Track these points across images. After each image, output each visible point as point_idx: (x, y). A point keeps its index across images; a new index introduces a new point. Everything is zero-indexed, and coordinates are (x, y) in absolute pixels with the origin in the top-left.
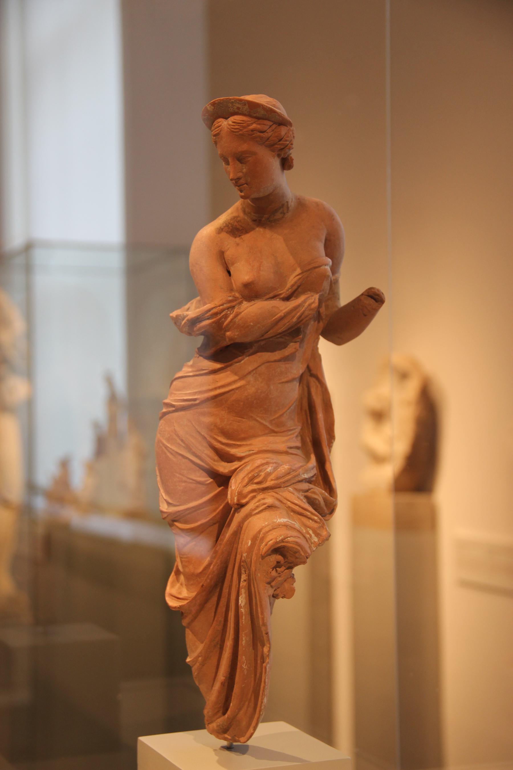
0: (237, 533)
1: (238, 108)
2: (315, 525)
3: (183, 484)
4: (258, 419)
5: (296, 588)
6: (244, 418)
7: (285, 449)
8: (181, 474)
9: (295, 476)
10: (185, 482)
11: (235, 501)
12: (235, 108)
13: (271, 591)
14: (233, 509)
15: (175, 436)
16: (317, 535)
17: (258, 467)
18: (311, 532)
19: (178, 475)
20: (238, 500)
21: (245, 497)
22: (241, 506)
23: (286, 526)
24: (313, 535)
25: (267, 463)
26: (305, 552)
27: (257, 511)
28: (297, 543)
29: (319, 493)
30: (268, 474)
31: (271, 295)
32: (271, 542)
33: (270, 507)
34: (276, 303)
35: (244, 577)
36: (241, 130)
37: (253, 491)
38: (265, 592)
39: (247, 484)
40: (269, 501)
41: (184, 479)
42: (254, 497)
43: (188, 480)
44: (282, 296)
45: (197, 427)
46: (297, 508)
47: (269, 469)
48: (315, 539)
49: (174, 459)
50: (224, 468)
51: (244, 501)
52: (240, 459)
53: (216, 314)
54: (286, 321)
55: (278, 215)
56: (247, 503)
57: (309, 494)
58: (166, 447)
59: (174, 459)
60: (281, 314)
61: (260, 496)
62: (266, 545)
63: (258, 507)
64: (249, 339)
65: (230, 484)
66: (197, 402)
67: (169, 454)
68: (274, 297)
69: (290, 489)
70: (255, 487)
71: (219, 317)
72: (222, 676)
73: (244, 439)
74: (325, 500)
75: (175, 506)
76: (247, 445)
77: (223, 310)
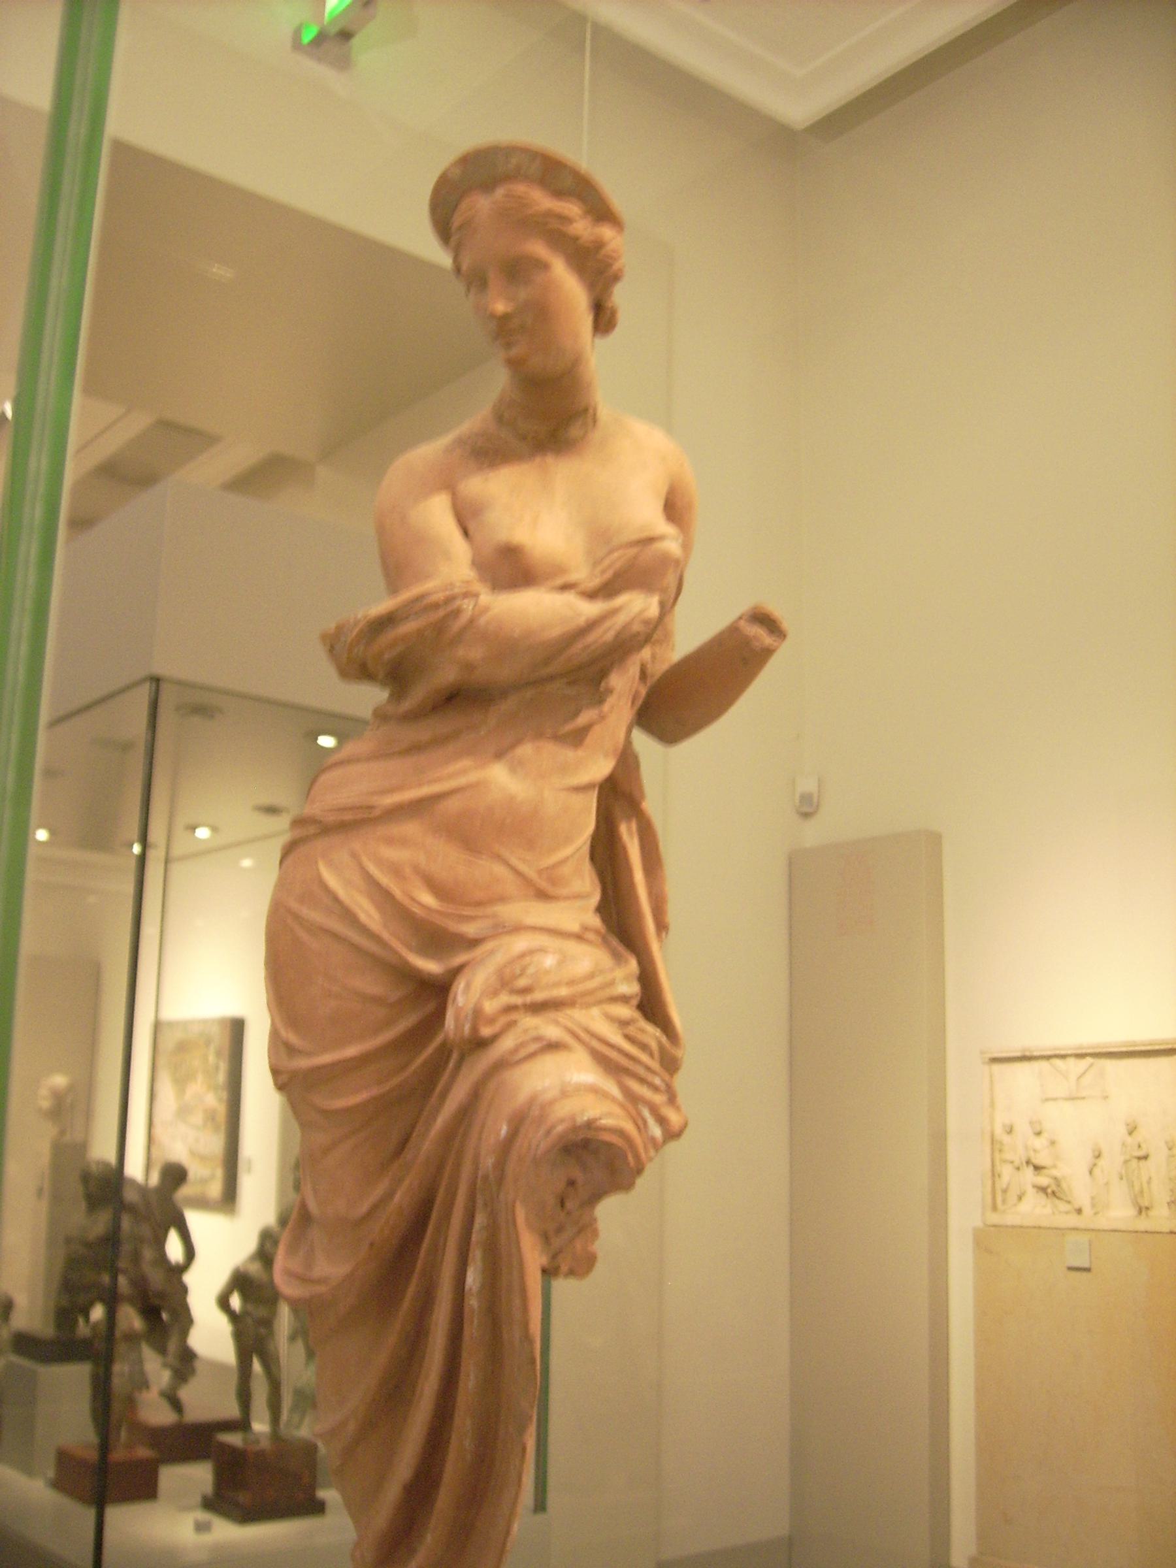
0: (466, 1113)
2: (659, 1099)
4: (514, 861)
5: (600, 1255)
7: (575, 927)
9: (604, 986)
11: (467, 1029)
13: (544, 1260)
14: (455, 1056)
16: (662, 1121)
17: (523, 955)
18: (646, 1113)
20: (475, 1029)
21: (491, 1021)
22: (480, 1044)
23: (594, 1090)
24: (651, 1122)
25: (542, 950)
26: (637, 1157)
28: (621, 1133)
29: (651, 1033)
30: (547, 972)
31: (559, 581)
32: (560, 1128)
33: (553, 1046)
34: (570, 598)
35: (480, 1220)
37: (510, 1009)
38: (533, 1257)
39: (495, 993)
40: (552, 1032)
42: (511, 1025)
44: (582, 587)
46: (614, 1055)
47: (549, 961)
48: (656, 1131)
51: (486, 1031)
52: (474, 943)
53: (436, 606)
54: (591, 638)
55: (575, 431)
56: (494, 1038)
57: (631, 1030)
58: (297, 917)
60: (582, 621)
61: (529, 1022)
62: (548, 1132)
63: (522, 1045)
64: (505, 673)
65: (451, 996)
66: (377, 812)
67: (303, 935)
68: (565, 587)
69: (595, 1011)
70: (517, 1000)
71: (441, 613)
72: (404, 1467)
73: (479, 904)
74: (662, 1048)
75: (309, 1054)
76: (487, 917)
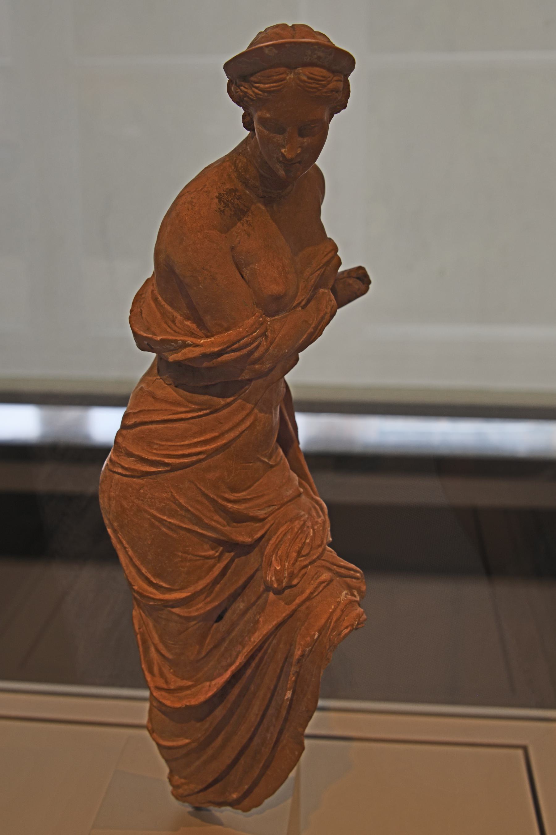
1: (319, 58)
3: (188, 564)
6: (251, 463)
8: (184, 553)
10: (191, 560)
12: (315, 56)
15: (174, 506)
19: (180, 554)
27: (316, 593)
36: (319, 90)
41: (190, 557)
43: (194, 558)
45: (203, 489)
49: (175, 535)
50: (243, 537)
51: (295, 582)
58: (161, 521)
59: (175, 535)
63: (316, 588)
77: (256, 338)
